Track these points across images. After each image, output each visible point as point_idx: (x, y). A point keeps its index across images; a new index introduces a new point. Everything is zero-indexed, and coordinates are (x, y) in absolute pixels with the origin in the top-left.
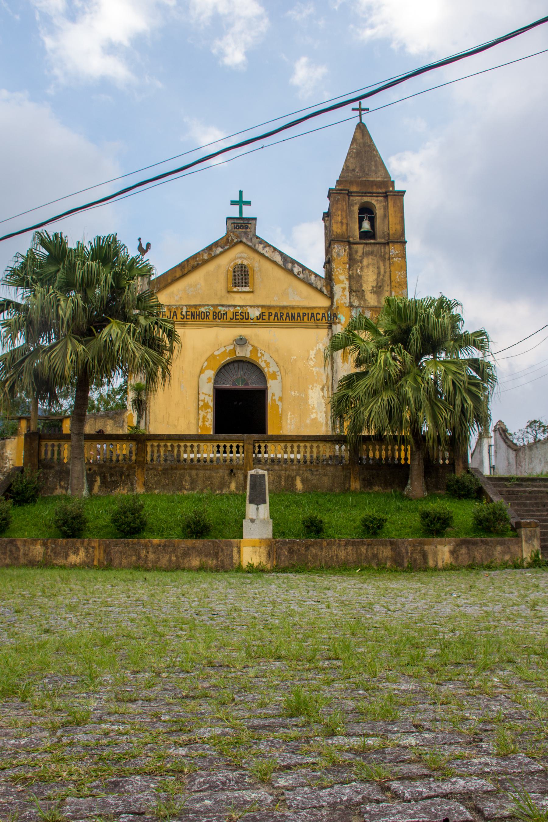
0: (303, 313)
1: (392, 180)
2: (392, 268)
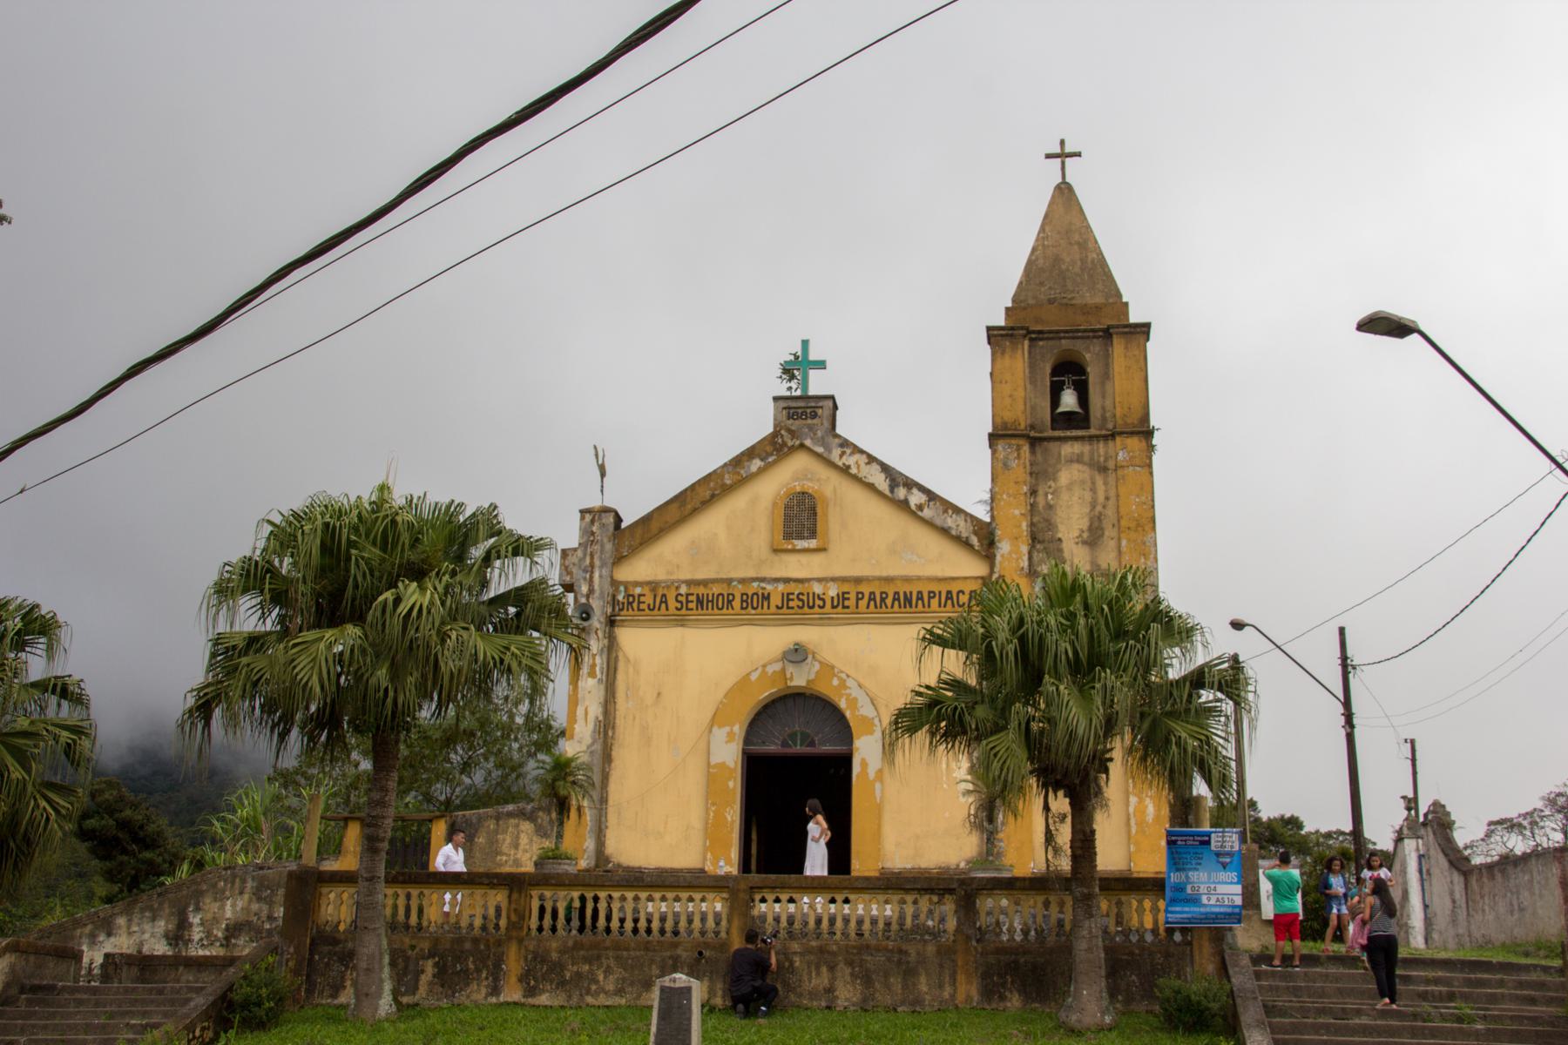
0: (930, 592)
1: (1124, 300)
2: (1122, 490)
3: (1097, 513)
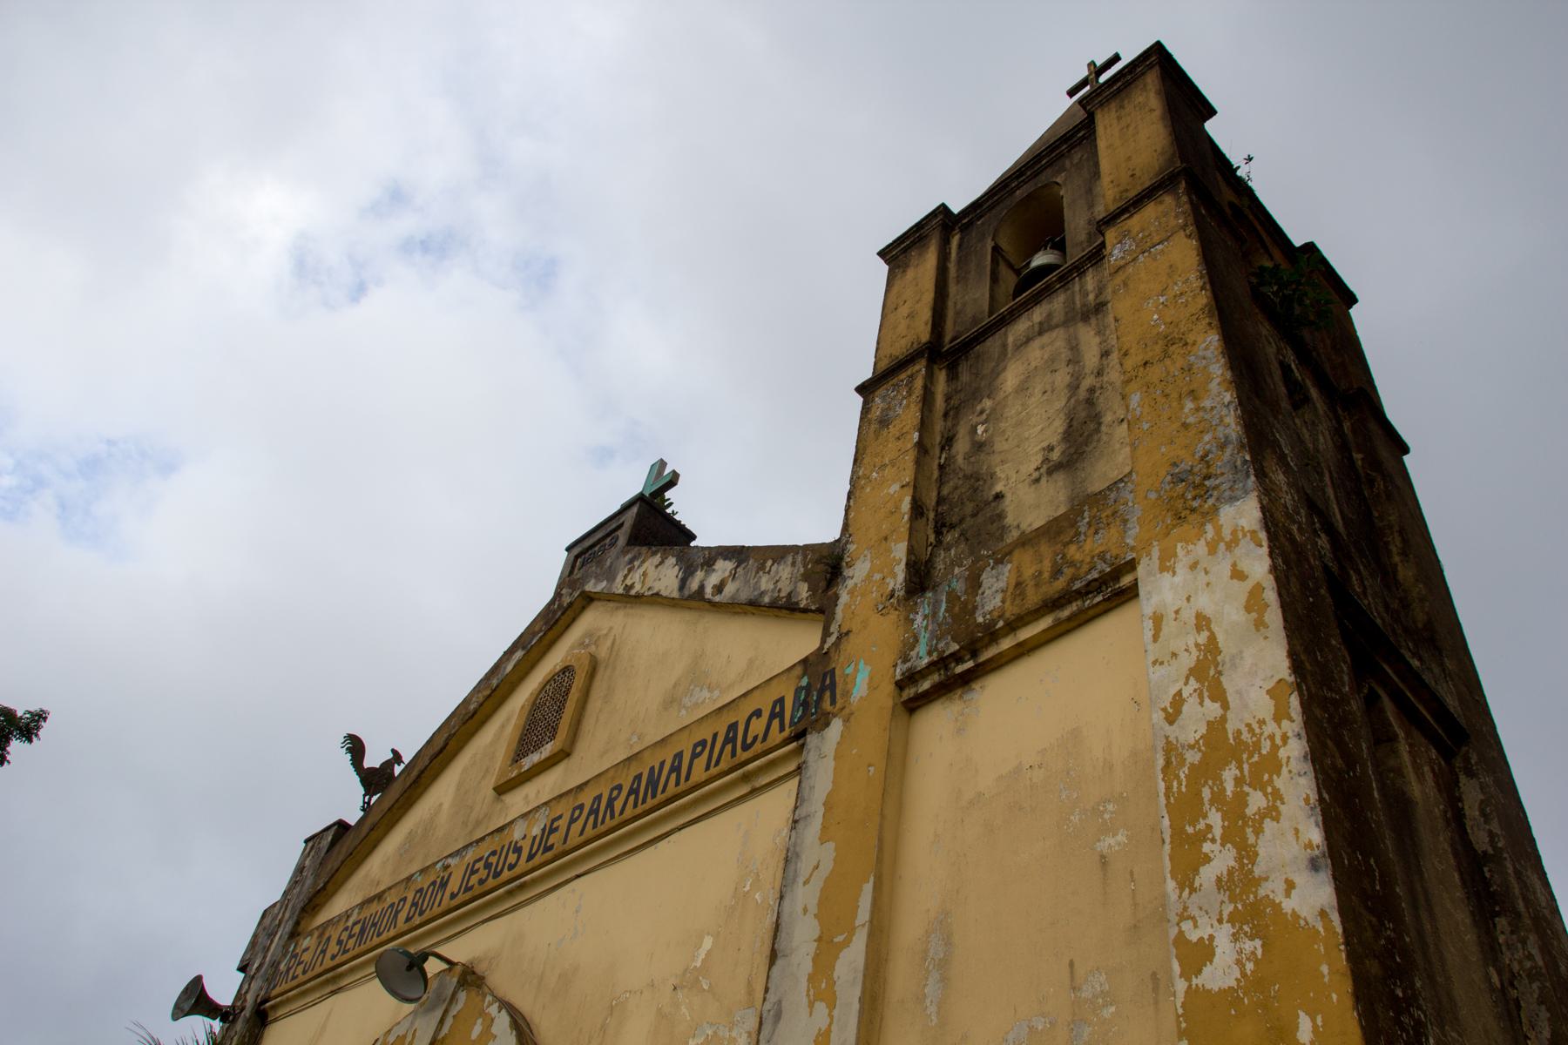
3: (1082, 393)
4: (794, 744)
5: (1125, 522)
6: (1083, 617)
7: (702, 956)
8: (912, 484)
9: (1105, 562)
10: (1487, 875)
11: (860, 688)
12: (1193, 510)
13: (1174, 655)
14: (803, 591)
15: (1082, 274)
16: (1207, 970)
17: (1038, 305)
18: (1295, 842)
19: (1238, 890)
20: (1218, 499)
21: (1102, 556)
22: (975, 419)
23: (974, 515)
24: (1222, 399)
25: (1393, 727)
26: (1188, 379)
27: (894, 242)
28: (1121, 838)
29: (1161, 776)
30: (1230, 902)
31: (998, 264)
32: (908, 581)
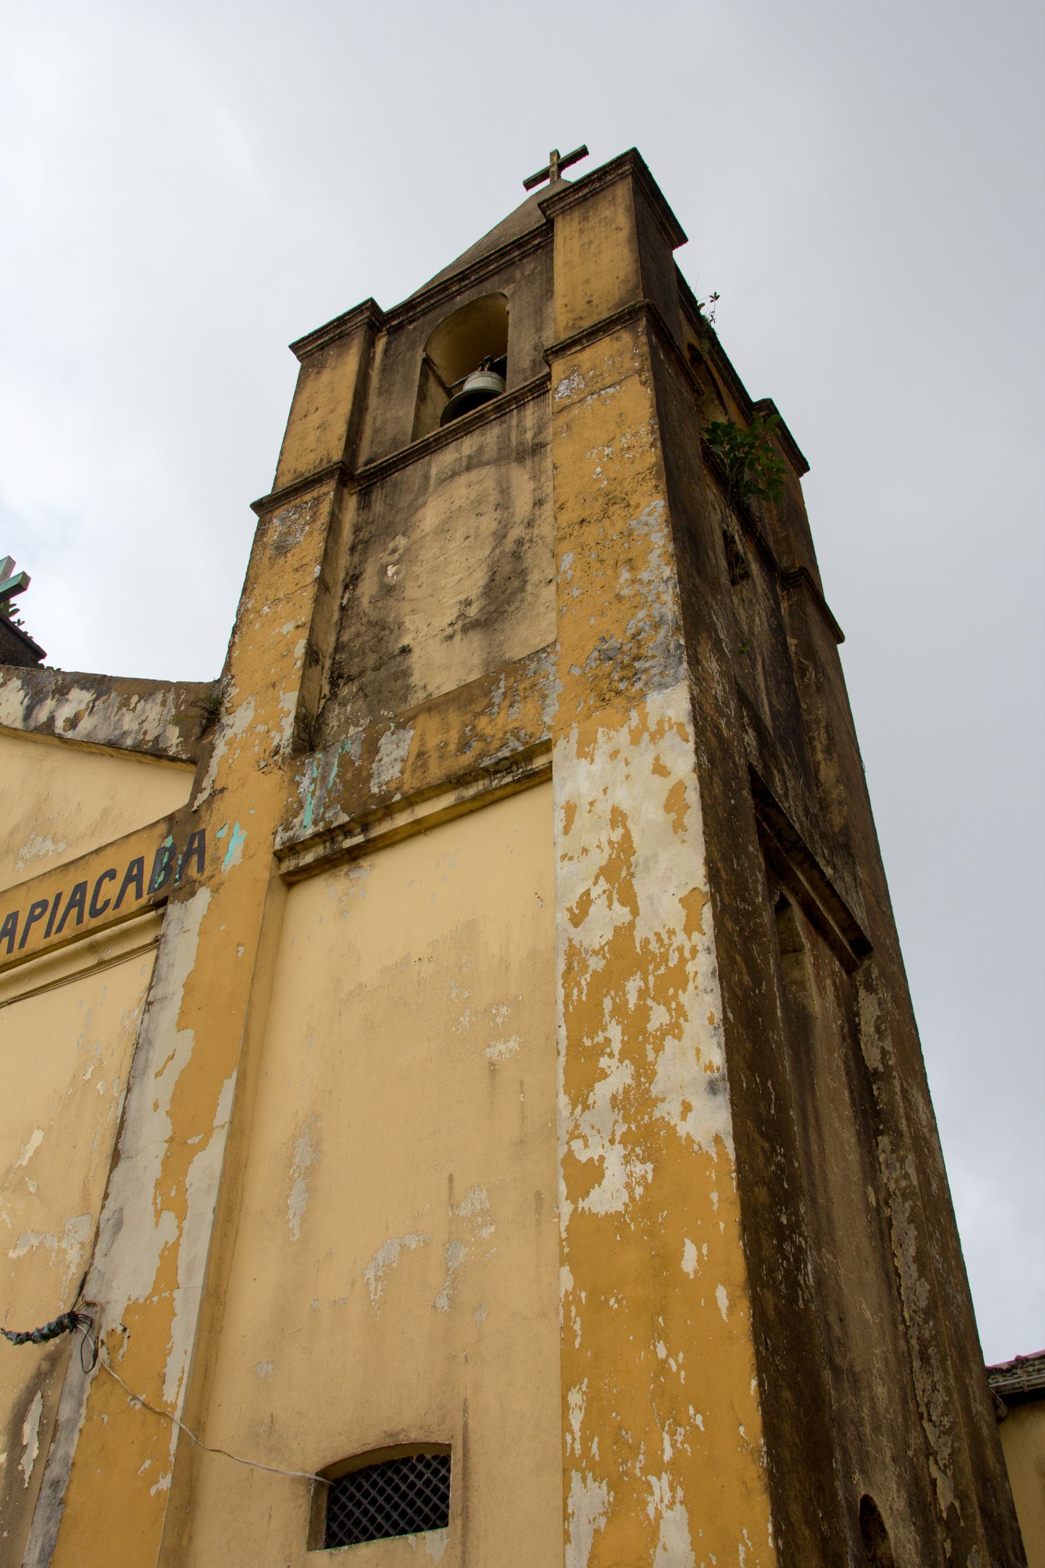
3: (509, 544)
4: (152, 914)
5: (544, 697)
6: (490, 798)
7: (30, 1153)
8: (308, 625)
9: (518, 740)
10: (876, 1093)
11: (233, 856)
12: (618, 693)
13: (585, 851)
14: (173, 738)
15: (521, 407)
16: (595, 1193)
17: (469, 436)
18: (695, 1063)
19: (633, 1110)
20: (646, 684)
21: (515, 733)
22: (386, 558)
23: (376, 669)
24: (662, 573)
25: (800, 937)
26: (626, 545)
27: (311, 335)
28: (513, 1044)
29: (561, 982)
30: (624, 1122)
31: (427, 379)
32: (296, 737)
